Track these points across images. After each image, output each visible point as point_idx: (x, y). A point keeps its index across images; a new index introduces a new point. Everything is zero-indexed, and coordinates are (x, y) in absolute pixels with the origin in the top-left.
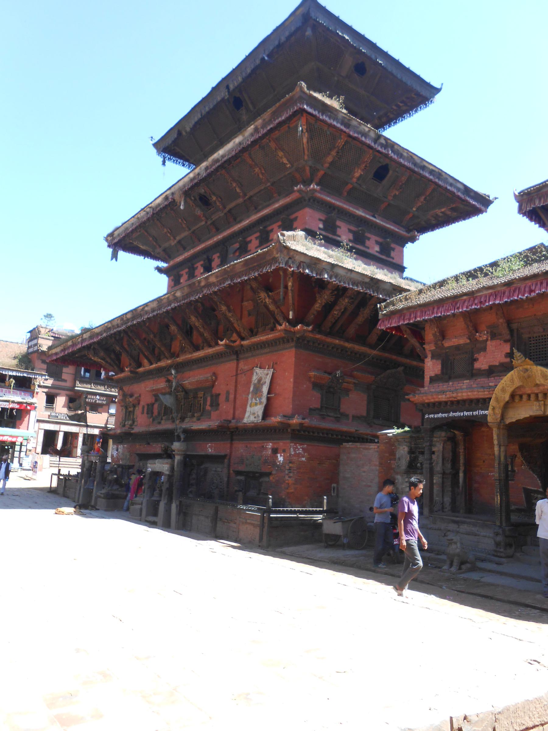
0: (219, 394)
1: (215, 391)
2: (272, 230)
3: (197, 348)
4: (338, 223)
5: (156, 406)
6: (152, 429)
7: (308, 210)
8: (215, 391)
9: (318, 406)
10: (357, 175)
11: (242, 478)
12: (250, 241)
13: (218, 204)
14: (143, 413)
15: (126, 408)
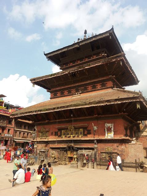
0: (91, 130)
1: (89, 129)
2: (97, 85)
3: (79, 116)
4: (115, 85)
5: (59, 132)
6: (60, 140)
7: (111, 82)
8: (89, 129)
9: (125, 134)
10: (120, 74)
11: (105, 154)
12: (88, 87)
13: (78, 76)
14: (52, 134)
15: (42, 132)
